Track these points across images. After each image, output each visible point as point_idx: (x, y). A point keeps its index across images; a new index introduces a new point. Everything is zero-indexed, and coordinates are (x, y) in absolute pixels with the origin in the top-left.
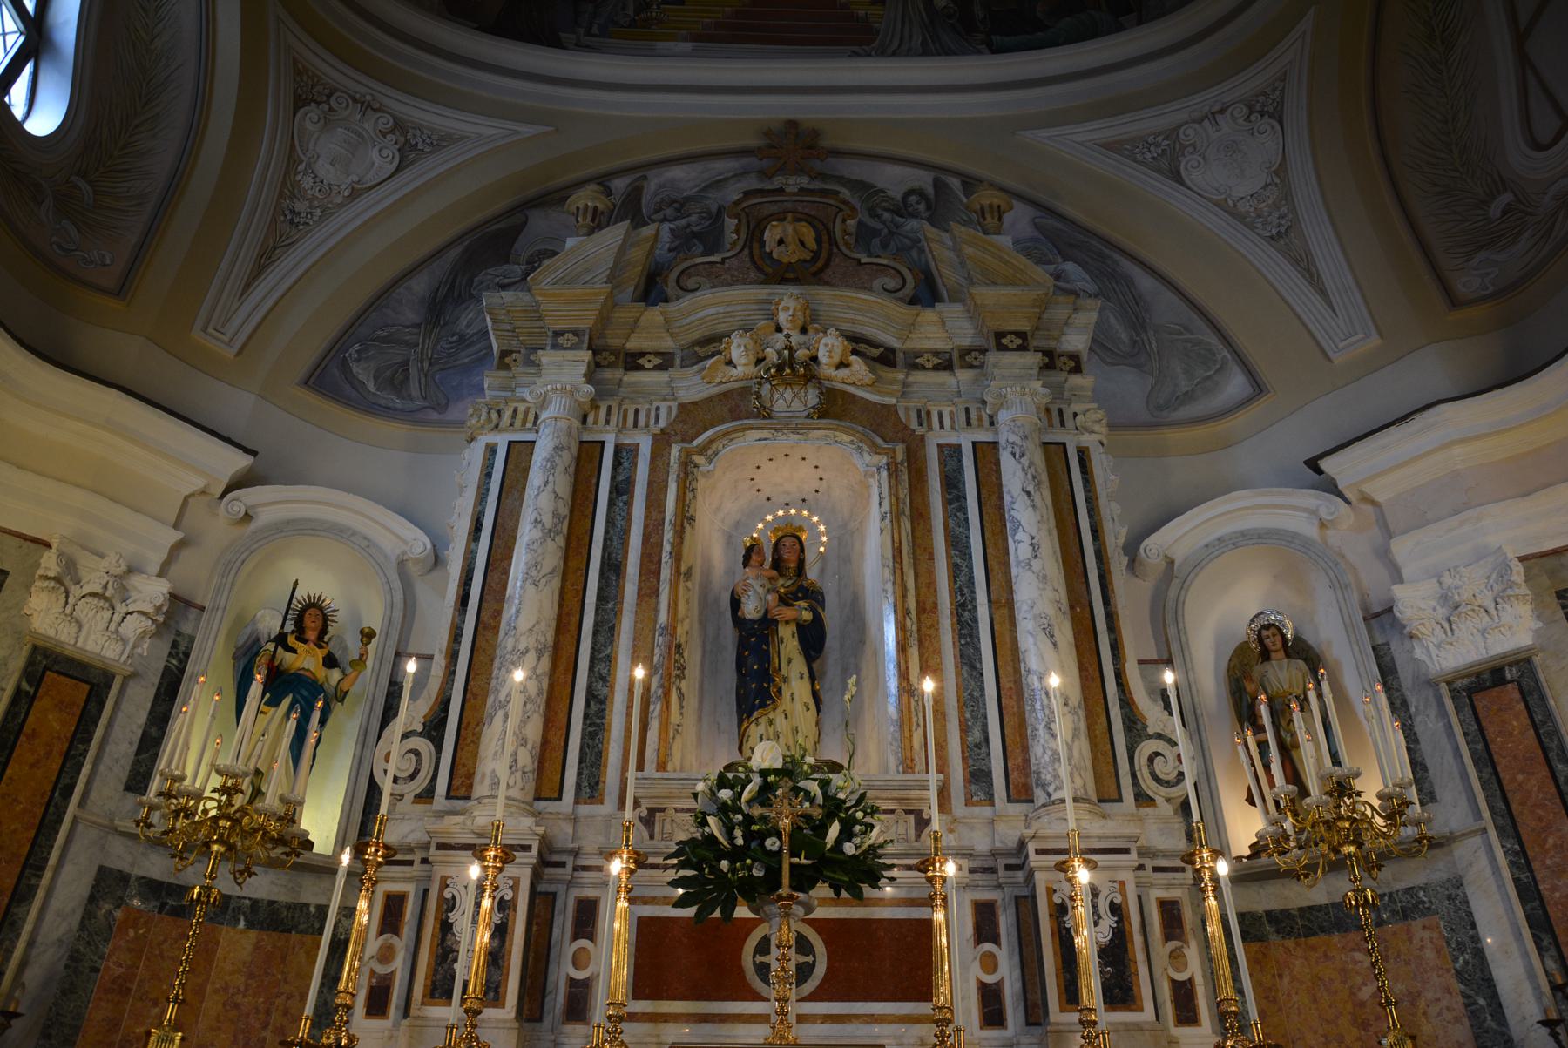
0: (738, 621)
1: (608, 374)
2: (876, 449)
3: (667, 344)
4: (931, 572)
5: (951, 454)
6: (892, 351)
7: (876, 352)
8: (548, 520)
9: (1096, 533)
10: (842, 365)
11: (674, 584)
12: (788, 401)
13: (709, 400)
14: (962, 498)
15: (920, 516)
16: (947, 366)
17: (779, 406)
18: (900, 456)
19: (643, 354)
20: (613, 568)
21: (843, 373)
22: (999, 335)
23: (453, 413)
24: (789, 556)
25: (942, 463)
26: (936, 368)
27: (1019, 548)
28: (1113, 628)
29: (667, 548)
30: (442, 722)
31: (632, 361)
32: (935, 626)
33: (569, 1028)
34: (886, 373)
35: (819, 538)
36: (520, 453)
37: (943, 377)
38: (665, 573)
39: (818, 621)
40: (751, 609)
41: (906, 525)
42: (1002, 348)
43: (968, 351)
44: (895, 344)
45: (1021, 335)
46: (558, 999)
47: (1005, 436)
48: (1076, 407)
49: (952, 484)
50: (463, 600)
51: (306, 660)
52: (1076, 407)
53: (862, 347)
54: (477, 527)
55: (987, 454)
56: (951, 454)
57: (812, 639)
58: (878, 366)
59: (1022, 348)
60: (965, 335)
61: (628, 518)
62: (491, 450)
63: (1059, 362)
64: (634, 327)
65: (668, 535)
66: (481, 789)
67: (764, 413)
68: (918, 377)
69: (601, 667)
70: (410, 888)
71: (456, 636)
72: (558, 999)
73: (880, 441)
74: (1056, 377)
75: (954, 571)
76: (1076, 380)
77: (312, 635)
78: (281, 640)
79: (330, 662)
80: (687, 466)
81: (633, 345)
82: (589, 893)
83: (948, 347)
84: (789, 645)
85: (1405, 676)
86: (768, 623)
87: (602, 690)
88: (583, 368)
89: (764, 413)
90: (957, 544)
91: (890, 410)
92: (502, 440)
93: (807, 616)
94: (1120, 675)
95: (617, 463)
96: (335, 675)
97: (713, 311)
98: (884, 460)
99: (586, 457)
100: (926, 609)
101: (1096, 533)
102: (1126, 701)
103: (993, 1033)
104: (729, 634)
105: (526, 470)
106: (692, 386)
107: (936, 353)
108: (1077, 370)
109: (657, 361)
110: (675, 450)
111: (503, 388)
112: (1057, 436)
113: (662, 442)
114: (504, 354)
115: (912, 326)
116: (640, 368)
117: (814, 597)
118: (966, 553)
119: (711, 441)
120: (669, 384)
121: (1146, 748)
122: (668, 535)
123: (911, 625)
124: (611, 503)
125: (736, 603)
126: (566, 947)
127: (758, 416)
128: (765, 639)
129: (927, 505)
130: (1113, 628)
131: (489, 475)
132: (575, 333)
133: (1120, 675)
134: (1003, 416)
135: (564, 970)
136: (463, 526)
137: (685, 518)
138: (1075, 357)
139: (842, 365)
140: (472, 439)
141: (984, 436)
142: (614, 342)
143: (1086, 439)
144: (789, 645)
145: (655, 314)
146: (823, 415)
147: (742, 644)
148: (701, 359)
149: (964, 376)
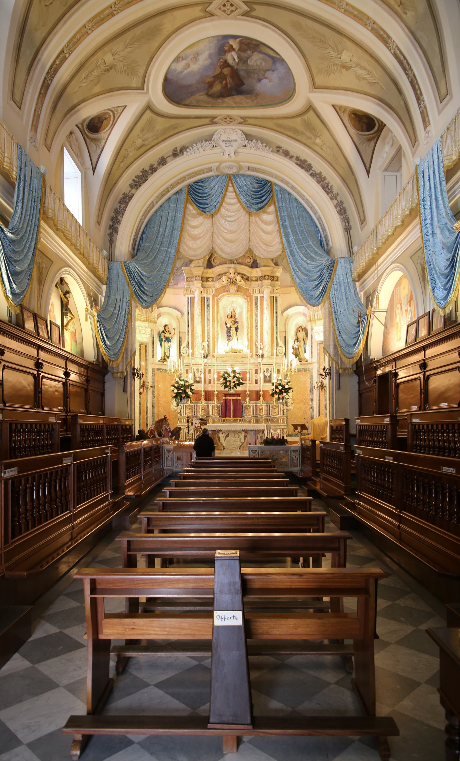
0: (227, 327)
1: (204, 283)
2: (245, 299)
3: (213, 276)
4: (252, 321)
5: (257, 298)
6: (248, 277)
7: (246, 277)
8: (199, 314)
9: (276, 313)
10: (240, 281)
11: (217, 324)
12: (233, 288)
13: (220, 288)
14: (257, 307)
15: (251, 310)
16: (257, 280)
17: (231, 290)
18: (249, 300)
19: (209, 278)
20: (208, 320)
21: (240, 283)
22: (265, 276)
23: (179, 286)
24: (233, 316)
25: (255, 300)
26: (255, 280)
27: (265, 318)
28: (276, 330)
29: (216, 317)
30: (189, 345)
31: (207, 279)
32: (252, 330)
33: (210, 385)
34: (248, 283)
35: (237, 312)
36: (193, 298)
37: (256, 282)
38: (216, 321)
39: (237, 327)
40: (228, 326)
41: (249, 313)
42: (265, 279)
43: (261, 277)
44: (249, 275)
45: (268, 276)
46: (208, 381)
47: (265, 297)
48: (277, 288)
49: (256, 304)
50: (188, 326)
51: (167, 335)
52: (277, 288)
53: (244, 276)
54: (188, 313)
55: (262, 298)
56: (257, 298)
57: (237, 329)
58: (246, 281)
59: (268, 279)
60: (260, 275)
61: (210, 311)
62: (188, 298)
63: (275, 279)
64: (207, 273)
65: (216, 315)
66: (195, 356)
67: (228, 291)
68: (252, 283)
69: (208, 337)
70: (189, 369)
71: (188, 332)
72: (208, 381)
73: (246, 297)
74: (274, 282)
75: (256, 320)
76: (277, 282)
77: (167, 330)
78: (163, 332)
79: (170, 334)
80: (218, 302)
81: (208, 276)
82: (210, 368)
83: (257, 276)
84: (233, 330)
85: (313, 340)
86: (230, 327)
87: (209, 340)
88: (200, 284)
89: (228, 291)
90: (256, 315)
91: (247, 289)
92: (190, 296)
93: (236, 326)
94: (276, 337)
95: (207, 301)
96: (171, 335)
97: (220, 270)
98: (246, 301)
99: (203, 298)
100: (251, 327)
101: (276, 313)
102: (277, 341)
103: (256, 385)
104: (226, 329)
105: (194, 303)
106: (217, 285)
107: (255, 277)
108: (278, 280)
109: (211, 279)
110: (216, 298)
111: (188, 285)
112: (272, 295)
113: (214, 296)
114: (187, 278)
115: (251, 272)
116: (209, 281)
117: (237, 322)
118: (257, 317)
119: (221, 297)
120: (214, 284)
121: (279, 348)
122: (216, 315)
123: (249, 330)
124: (207, 308)
125: (226, 324)
126: (208, 375)
127: (227, 292)
128: (230, 330)
129: (252, 308)
130: (276, 330)
131: (188, 303)
132: (199, 276)
133: (276, 337)
134: (264, 292)
135: (208, 378)
136: (186, 313)
137: (218, 312)
138: (278, 277)
139: (240, 281)
140: (185, 296)
141: (261, 295)
142: (204, 276)
143: (278, 295)
144: (233, 330)
145: (210, 270)
146: (237, 291)
147: (227, 331)
148: (218, 279)
149: (259, 283)
